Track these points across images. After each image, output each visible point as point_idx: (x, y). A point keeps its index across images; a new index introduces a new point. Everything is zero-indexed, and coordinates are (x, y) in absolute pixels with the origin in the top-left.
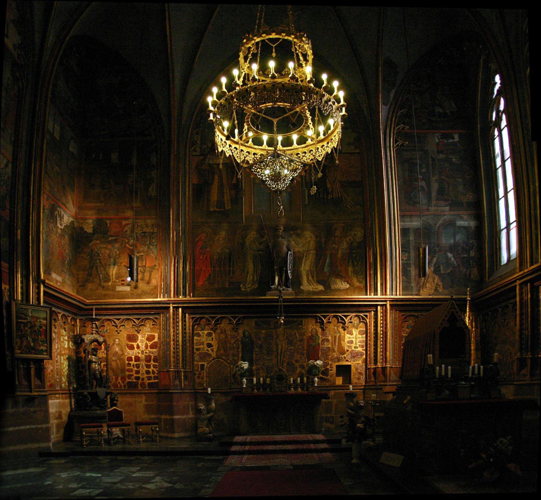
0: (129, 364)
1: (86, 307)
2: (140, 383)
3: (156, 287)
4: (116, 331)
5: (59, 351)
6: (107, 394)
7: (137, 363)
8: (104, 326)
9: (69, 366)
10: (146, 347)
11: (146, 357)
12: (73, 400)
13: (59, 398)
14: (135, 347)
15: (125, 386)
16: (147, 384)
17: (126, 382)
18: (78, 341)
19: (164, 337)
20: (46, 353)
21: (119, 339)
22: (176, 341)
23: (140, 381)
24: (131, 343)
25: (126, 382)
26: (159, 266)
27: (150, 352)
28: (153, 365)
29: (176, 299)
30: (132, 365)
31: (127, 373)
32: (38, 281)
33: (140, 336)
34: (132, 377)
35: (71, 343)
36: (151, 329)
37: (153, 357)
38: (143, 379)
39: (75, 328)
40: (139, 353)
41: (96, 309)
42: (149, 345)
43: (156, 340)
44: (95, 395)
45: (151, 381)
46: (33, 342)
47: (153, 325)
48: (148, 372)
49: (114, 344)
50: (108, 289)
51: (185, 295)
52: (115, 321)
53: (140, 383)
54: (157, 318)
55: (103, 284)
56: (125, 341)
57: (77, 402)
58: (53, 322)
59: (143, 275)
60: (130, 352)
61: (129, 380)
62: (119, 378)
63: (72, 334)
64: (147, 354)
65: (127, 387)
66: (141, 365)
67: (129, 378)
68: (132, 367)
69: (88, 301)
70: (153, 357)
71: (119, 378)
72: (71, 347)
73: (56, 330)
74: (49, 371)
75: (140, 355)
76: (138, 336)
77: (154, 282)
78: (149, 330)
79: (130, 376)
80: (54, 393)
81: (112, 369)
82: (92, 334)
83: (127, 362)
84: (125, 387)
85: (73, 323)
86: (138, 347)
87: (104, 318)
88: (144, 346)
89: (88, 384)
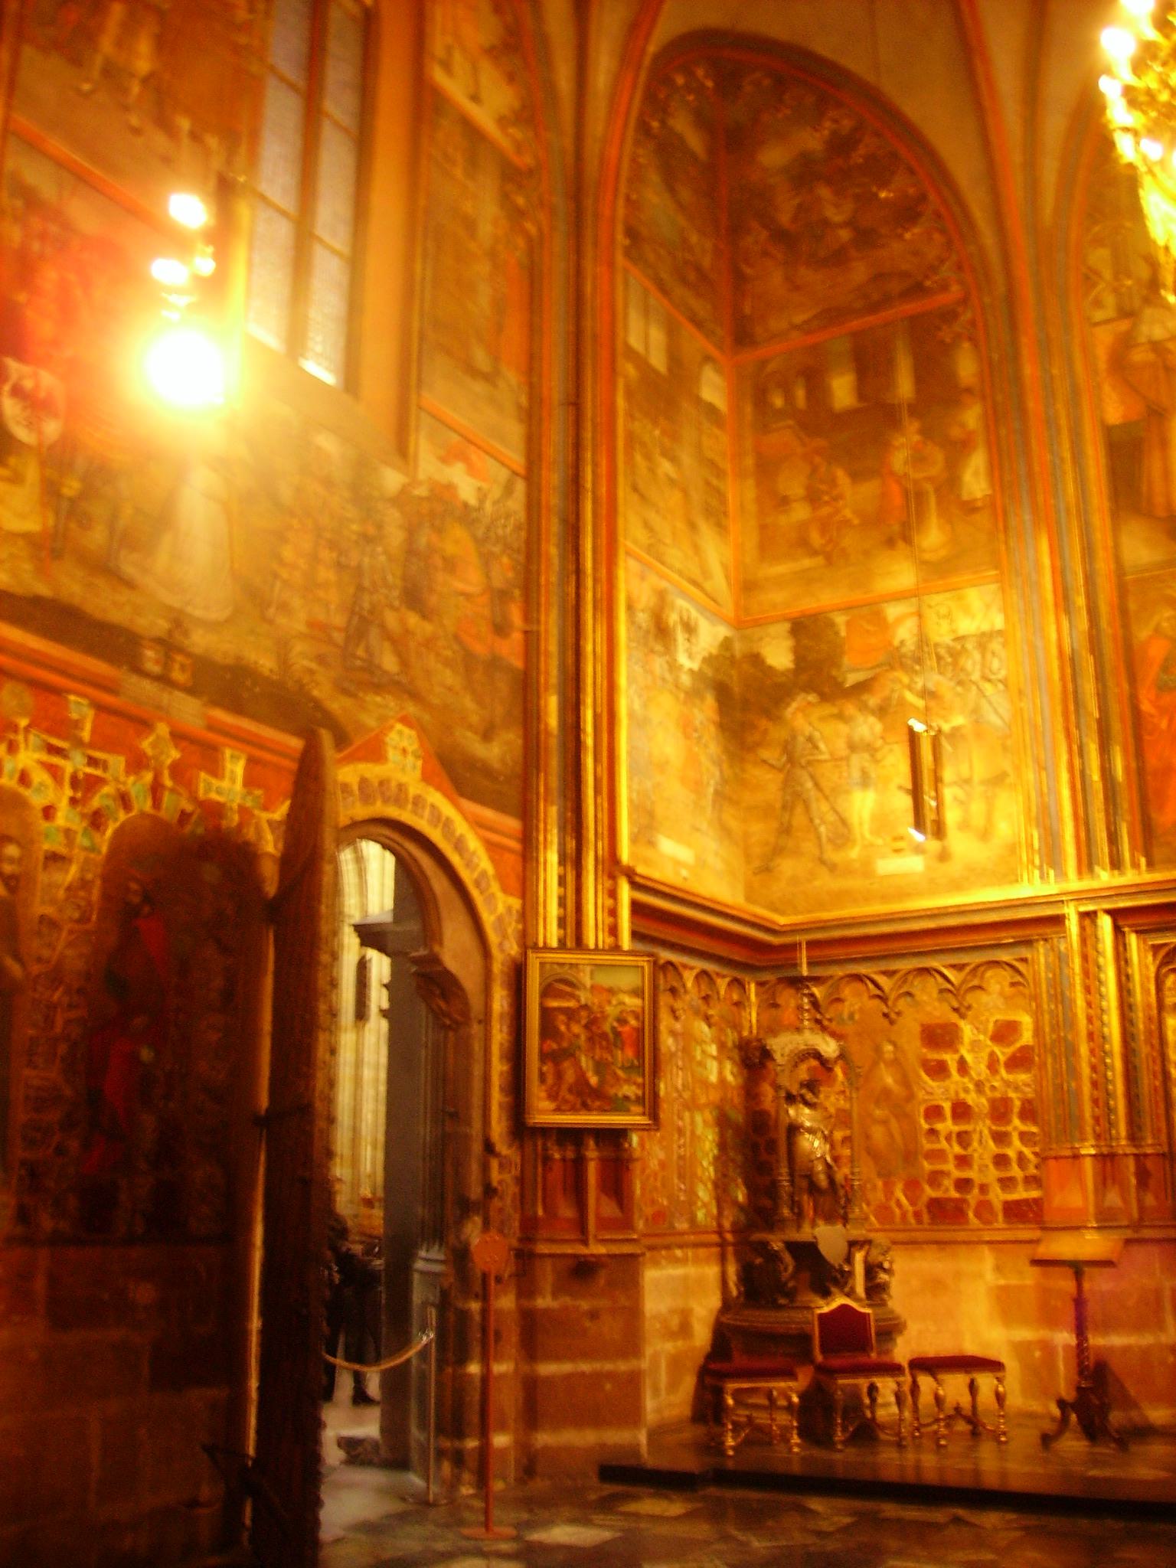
0: (932, 1132)
1: (775, 940)
3: (1012, 849)
4: (886, 1015)
6: (853, 1244)
8: (839, 1000)
9: (722, 1146)
10: (992, 1065)
11: (993, 1102)
12: (732, 1270)
13: (683, 1261)
15: (917, 1215)
16: (998, 1207)
17: (924, 1199)
18: (753, 1059)
19: (1055, 1027)
21: (894, 1044)
22: (1096, 1038)
23: (973, 1197)
27: (1007, 1084)
29: (1087, 884)
31: (927, 1166)
32: (612, 867)
33: (967, 1030)
34: (948, 1183)
35: (728, 1067)
36: (1006, 998)
37: (1017, 1104)
38: (984, 1188)
40: (966, 1090)
41: (812, 945)
42: (1002, 1058)
43: (1027, 1037)
44: (807, 1253)
47: (1013, 984)
48: (1001, 1161)
49: (875, 1064)
50: (848, 871)
51: (1116, 864)
52: (882, 980)
54: (1024, 960)
55: (831, 855)
56: (914, 1048)
57: (747, 1275)
58: (665, 999)
63: (731, 1037)
64: (998, 1095)
65: (926, 1217)
66: (976, 1137)
68: (944, 1144)
69: (782, 920)
72: (730, 1078)
73: (678, 1026)
74: (654, 1164)
75: (971, 1099)
78: (1000, 1002)
79: (935, 1178)
80: (664, 1240)
81: (874, 1154)
82: (799, 1030)
83: (925, 1126)
85: (735, 997)
86: (963, 1067)
87: (838, 971)
89: (786, 1212)
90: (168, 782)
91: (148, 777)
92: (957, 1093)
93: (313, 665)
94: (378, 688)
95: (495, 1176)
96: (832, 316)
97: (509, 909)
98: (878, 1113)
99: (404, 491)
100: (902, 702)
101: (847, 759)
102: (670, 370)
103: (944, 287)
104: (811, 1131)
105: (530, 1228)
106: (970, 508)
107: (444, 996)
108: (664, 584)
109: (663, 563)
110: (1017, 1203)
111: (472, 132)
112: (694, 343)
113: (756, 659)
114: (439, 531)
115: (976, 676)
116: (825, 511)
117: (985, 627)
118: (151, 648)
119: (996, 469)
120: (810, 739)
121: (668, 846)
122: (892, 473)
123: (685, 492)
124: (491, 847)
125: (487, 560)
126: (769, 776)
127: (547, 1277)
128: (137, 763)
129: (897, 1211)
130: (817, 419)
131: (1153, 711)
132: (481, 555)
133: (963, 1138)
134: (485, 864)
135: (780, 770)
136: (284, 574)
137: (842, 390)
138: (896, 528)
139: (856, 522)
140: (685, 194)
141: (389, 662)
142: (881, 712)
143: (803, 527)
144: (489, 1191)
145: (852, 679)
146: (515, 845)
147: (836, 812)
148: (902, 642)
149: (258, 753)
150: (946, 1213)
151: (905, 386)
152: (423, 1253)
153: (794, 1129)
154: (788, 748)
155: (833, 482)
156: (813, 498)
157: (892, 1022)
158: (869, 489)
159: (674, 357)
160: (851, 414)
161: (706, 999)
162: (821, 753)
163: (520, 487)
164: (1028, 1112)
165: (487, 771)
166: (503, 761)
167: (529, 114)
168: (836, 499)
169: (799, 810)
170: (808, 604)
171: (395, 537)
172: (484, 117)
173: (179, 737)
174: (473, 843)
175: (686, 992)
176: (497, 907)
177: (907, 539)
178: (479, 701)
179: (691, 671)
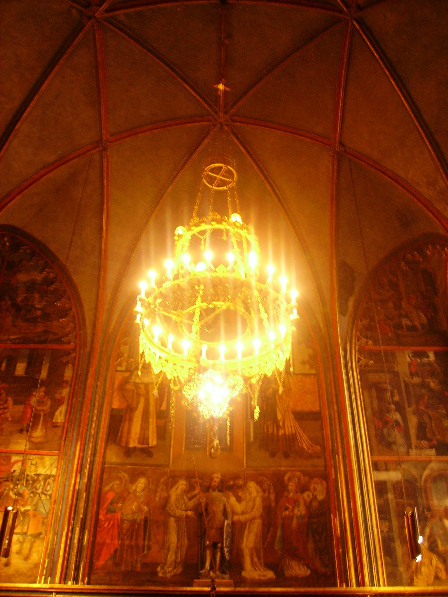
26: (46, 535)
59: (22, 546)
77: (35, 557)
96: (25, 341)
100: (8, 495)
103: (69, 342)
106: (55, 426)
115: (40, 491)
117: (48, 473)
119: (68, 413)
122: (29, 404)
131: (103, 519)
137: (20, 369)
139: (10, 419)
148: (15, 471)
151: (44, 374)
155: (6, 402)
158: (20, 408)
160: (21, 378)
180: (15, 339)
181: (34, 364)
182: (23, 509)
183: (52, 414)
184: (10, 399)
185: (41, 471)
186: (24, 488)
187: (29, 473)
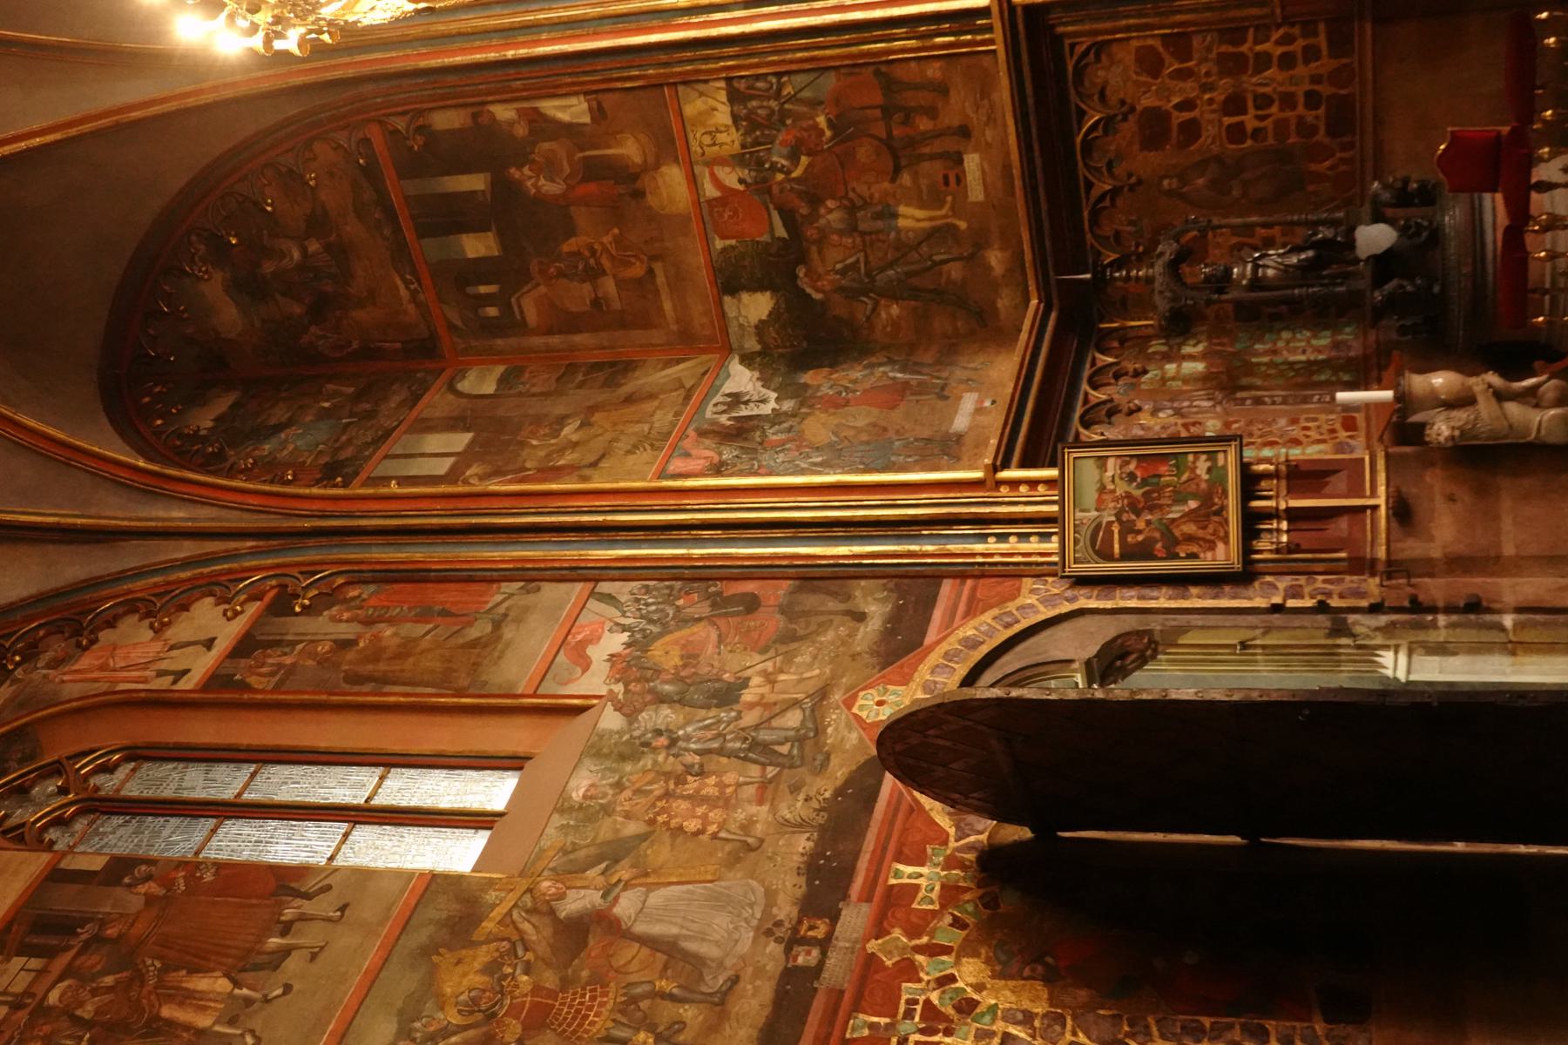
2: (1334, 90)
5: (1219, 395)
7: (1250, 104)
8: (1117, 234)
11: (1221, 74)
14: (1187, 115)
15: (1344, 148)
16: (1334, 64)
17: (1327, 141)
18: (1179, 325)
20: (1221, 456)
23: (1325, 89)
24: (1174, 133)
25: (1327, 141)
28: (1256, 42)
30: (1257, 124)
33: (1147, 101)
34: (1310, 116)
35: (1187, 350)
37: (1223, 48)
38: (1316, 79)
39: (1133, 334)
40: (1211, 101)
45: (1324, 46)
46: (1184, 501)
48: (1287, 61)
53: (1334, 90)
60: (1209, 132)
61: (1322, 131)
62: (1314, 167)
63: (1157, 346)
64: (1215, 70)
65: (1346, 139)
67: (1313, 130)
68: (1268, 123)
69: (1034, 302)
70: (1223, 48)
71: (1314, 167)
72: (1200, 348)
75: (1219, 96)
76: (1146, 109)
78: (1117, 70)
83: (1249, 143)
84: (1352, 146)
85: (1116, 344)
86: (1187, 105)
88: (1181, 84)
90: (925, 940)
91: (920, 958)
92: (1213, 111)
93: (801, 797)
94: (819, 731)
95: (1309, 603)
96: (401, 255)
97: (1032, 591)
98: (1236, 193)
99: (619, 708)
101: (863, 234)
102: (468, 430)
104: (1256, 267)
105: (1361, 565)
107: (1123, 656)
108: (691, 432)
109: (670, 433)
110: (1330, 42)
111: (245, 647)
112: (437, 402)
113: (761, 328)
114: (658, 672)
115: (773, 104)
116: (606, 262)
117: (723, 96)
118: (795, 959)
120: (843, 272)
121: (961, 422)
123: (593, 409)
124: (970, 612)
125: (684, 621)
126: (884, 315)
127: (1412, 548)
128: (909, 971)
129: (1343, 168)
130: (508, 272)
132: (679, 628)
133: (1263, 102)
134: (987, 617)
135: (876, 304)
136: (713, 828)
137: (476, 246)
138: (621, 189)
140: (280, 414)
141: (793, 719)
142: (815, 201)
143: (620, 284)
144: (1322, 608)
145: (781, 232)
146: (969, 583)
147: (920, 243)
148: (741, 181)
149: (892, 848)
150: (1342, 119)
151: (475, 182)
152: (1389, 673)
153: (1257, 283)
154: (852, 294)
155: (577, 254)
156: (594, 274)
157: (1140, 182)
158: (581, 216)
159: (453, 424)
160: (501, 235)
161: (1117, 376)
162: (858, 261)
163: (605, 587)
164: (1234, 34)
165: (894, 621)
166: (883, 601)
167: (220, 588)
168: (593, 253)
169: (915, 281)
170: (704, 277)
171: (666, 715)
172: (228, 633)
173: (879, 930)
174: (968, 631)
175: (1111, 400)
176: (1034, 601)
177: (635, 177)
178: (823, 627)
179: (777, 400)
180: (407, 283)
181: (454, 216)
182: (828, 133)
183: (570, 130)
184: (566, 248)
185: (723, 116)
186: (777, 147)
187: (737, 145)
